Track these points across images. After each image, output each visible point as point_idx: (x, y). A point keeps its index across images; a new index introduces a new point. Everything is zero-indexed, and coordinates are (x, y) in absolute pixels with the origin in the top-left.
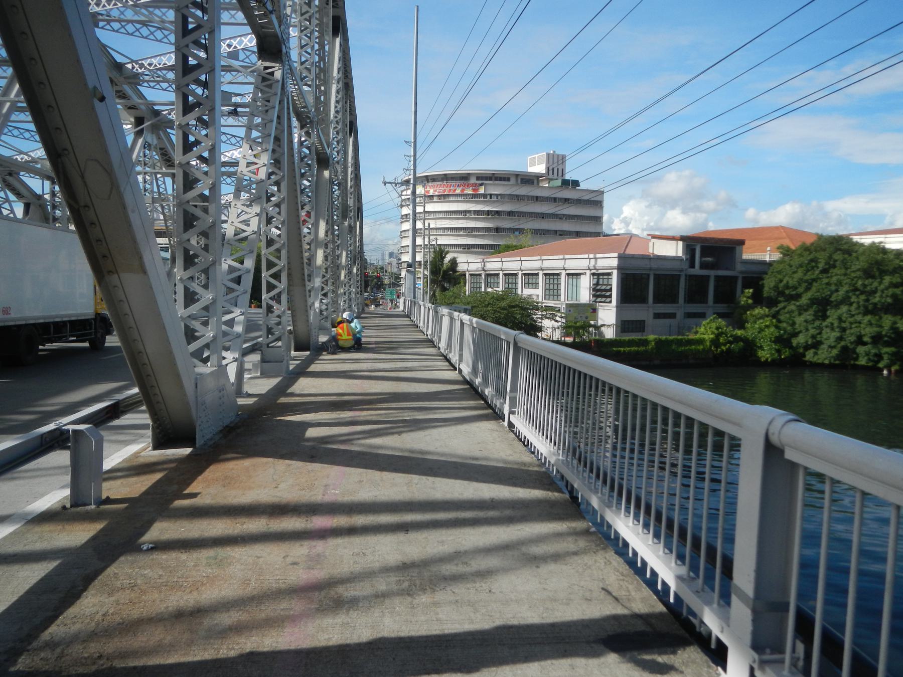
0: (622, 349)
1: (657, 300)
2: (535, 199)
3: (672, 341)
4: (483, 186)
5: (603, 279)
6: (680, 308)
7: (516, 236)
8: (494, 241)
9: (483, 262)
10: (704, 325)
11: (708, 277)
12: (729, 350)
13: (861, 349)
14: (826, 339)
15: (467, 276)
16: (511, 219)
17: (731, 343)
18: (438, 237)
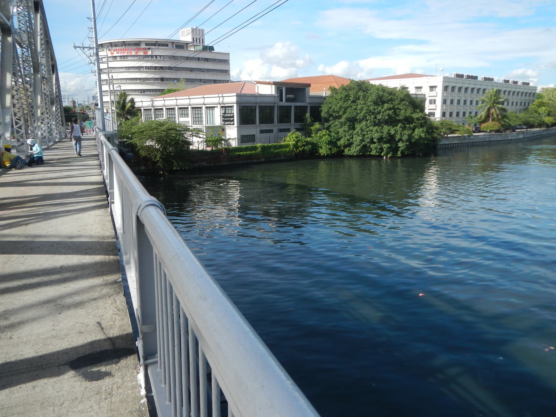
0: (242, 153)
1: (261, 122)
2: (186, 59)
3: (271, 146)
5: (228, 110)
6: (275, 126)
7: (174, 84)
9: (152, 101)
10: (289, 136)
11: (291, 107)
12: (303, 150)
13: (373, 146)
14: (355, 141)
15: (142, 110)
17: (304, 146)
18: (121, 85)
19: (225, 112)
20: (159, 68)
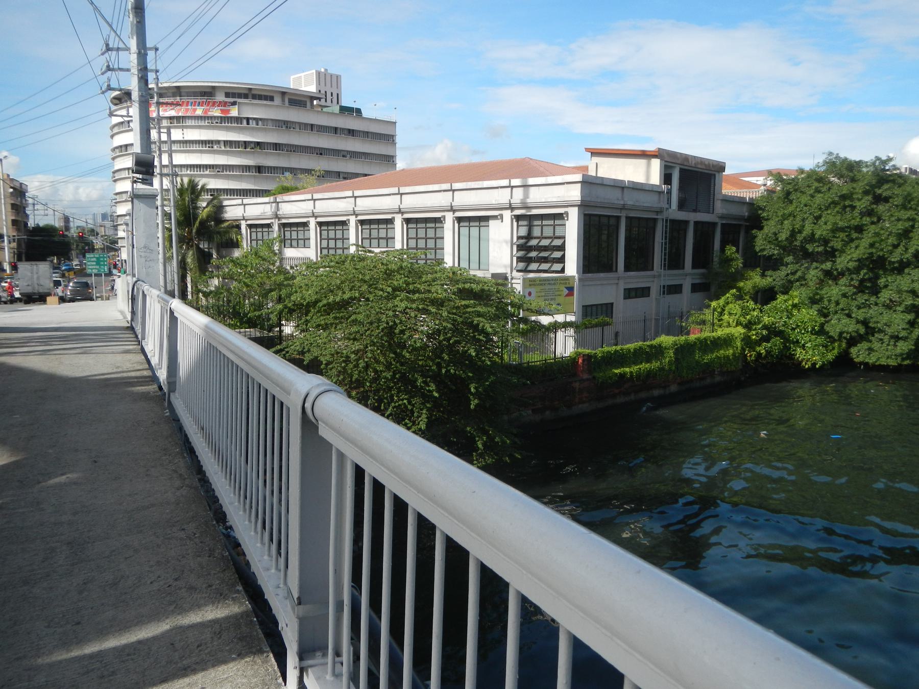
8: (255, 184)
20: (252, 145)
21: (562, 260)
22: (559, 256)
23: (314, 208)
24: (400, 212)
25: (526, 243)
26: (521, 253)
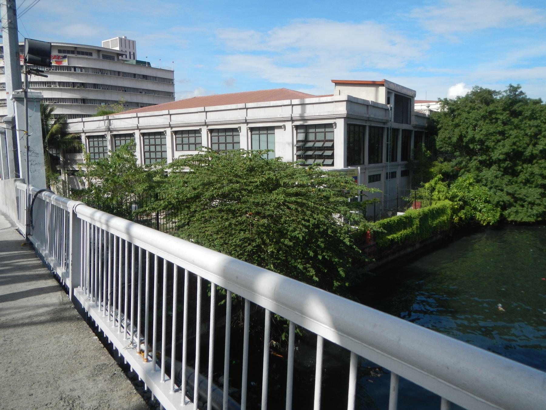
4: (67, 59)
16: (97, 91)
19: (306, 137)
20: (79, 85)
21: (332, 157)
22: (330, 154)
23: (139, 123)
24: (206, 124)
25: (305, 145)
26: (300, 153)
